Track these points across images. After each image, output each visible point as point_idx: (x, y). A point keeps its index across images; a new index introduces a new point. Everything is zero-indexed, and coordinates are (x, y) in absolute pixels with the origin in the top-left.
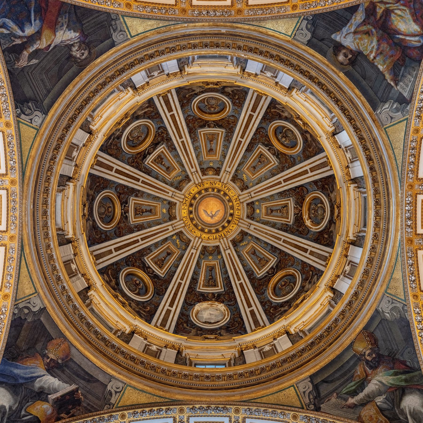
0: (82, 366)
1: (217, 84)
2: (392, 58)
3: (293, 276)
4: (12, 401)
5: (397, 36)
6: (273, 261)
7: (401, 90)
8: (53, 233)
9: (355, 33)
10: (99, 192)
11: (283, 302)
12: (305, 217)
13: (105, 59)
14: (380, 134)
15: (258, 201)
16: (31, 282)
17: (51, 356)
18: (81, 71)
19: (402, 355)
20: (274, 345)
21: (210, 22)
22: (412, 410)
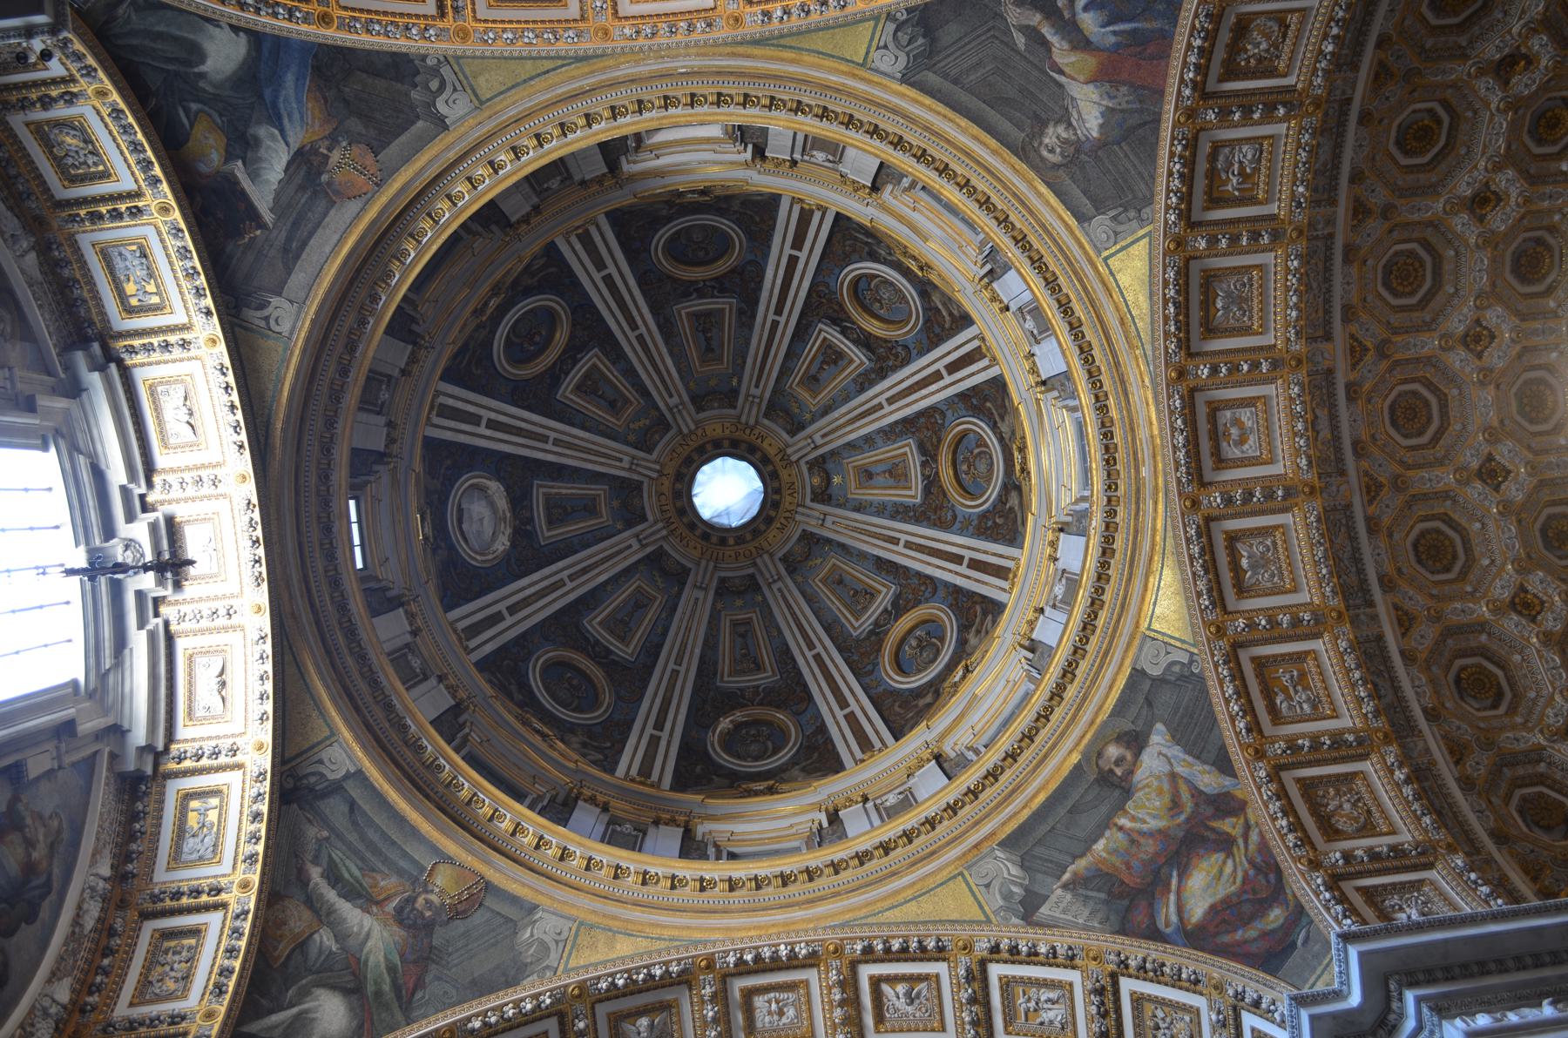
0: (320, 230)
1: (1023, 470)
2: (1124, 868)
3: (594, 703)
4: (219, 77)
5: (1175, 873)
6: (626, 651)
7: (1053, 898)
8: (627, 125)
9: (1173, 776)
10: (739, 223)
11: (530, 686)
12: (739, 716)
13: (1048, 203)
14: (947, 865)
15: (765, 599)
16: (503, 88)
17: (335, 156)
18: (1013, 152)
19: (439, 979)
20: (426, 678)
21: (1162, 438)
22: (314, 1015)
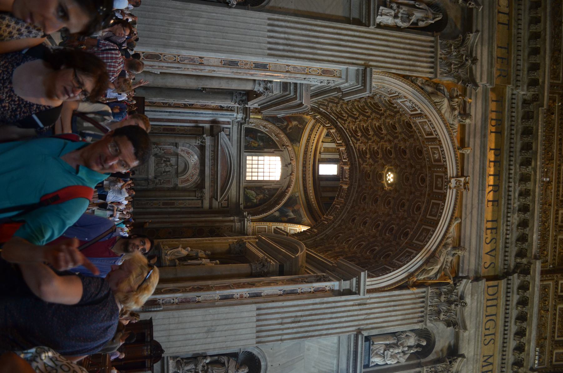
17: (295, 208)
